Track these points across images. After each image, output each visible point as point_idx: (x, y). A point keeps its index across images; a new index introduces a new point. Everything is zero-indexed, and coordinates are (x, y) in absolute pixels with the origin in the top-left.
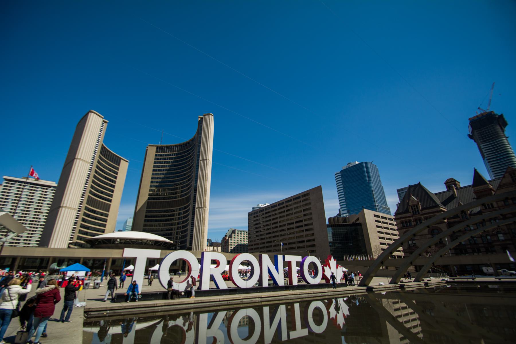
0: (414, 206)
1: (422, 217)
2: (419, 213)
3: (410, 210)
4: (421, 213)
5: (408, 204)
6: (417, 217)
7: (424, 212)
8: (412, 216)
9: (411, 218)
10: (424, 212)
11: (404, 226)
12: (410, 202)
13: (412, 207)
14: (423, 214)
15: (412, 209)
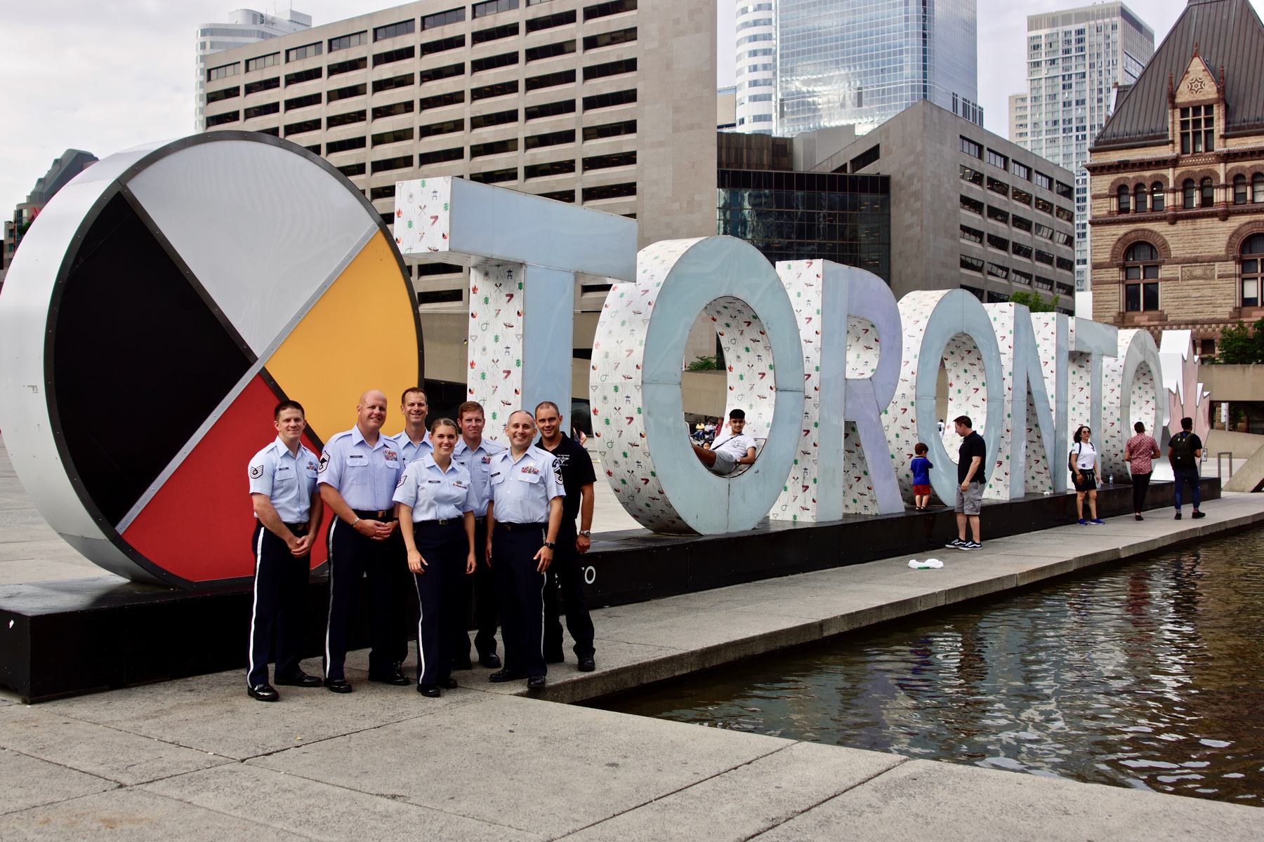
0: (1197, 110)
1: (1221, 169)
2: (1208, 148)
3: (1175, 132)
4: (1219, 146)
5: (1172, 96)
6: (1195, 167)
7: (1235, 145)
8: (1174, 163)
9: (1170, 174)
10: (1235, 145)
11: (1123, 210)
12: (1183, 88)
13: (1184, 112)
14: (1228, 157)
15: (1184, 124)
